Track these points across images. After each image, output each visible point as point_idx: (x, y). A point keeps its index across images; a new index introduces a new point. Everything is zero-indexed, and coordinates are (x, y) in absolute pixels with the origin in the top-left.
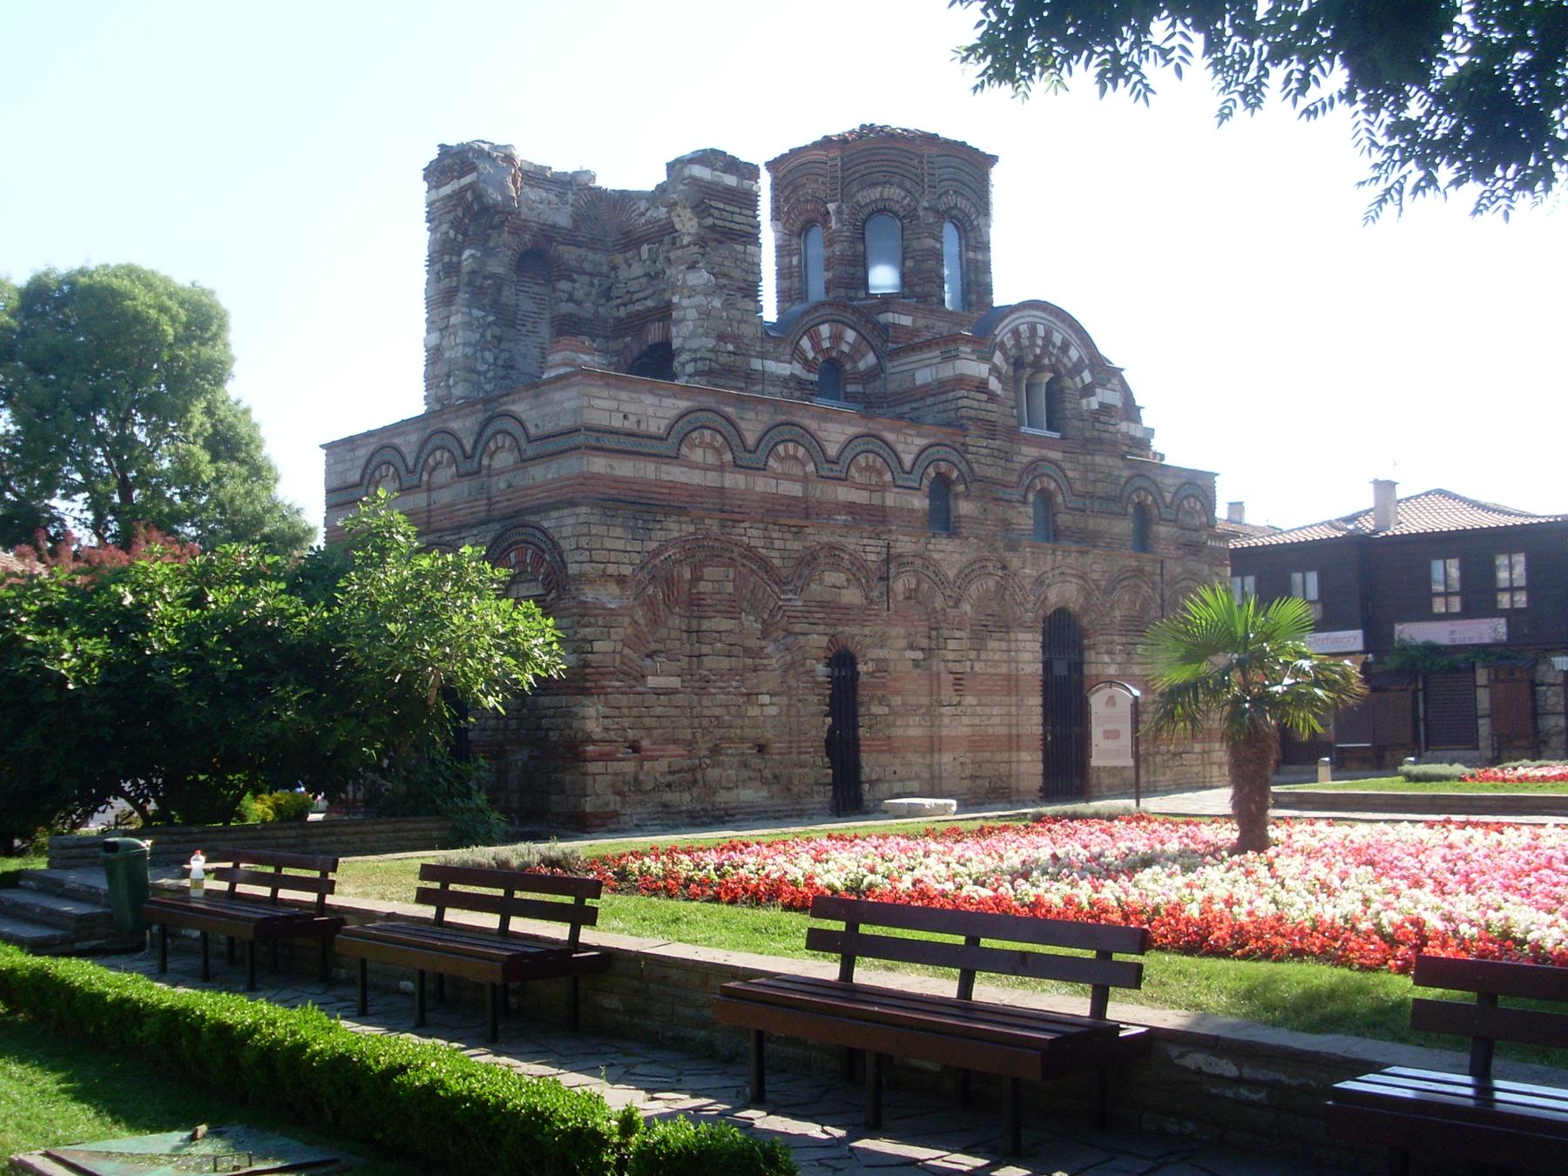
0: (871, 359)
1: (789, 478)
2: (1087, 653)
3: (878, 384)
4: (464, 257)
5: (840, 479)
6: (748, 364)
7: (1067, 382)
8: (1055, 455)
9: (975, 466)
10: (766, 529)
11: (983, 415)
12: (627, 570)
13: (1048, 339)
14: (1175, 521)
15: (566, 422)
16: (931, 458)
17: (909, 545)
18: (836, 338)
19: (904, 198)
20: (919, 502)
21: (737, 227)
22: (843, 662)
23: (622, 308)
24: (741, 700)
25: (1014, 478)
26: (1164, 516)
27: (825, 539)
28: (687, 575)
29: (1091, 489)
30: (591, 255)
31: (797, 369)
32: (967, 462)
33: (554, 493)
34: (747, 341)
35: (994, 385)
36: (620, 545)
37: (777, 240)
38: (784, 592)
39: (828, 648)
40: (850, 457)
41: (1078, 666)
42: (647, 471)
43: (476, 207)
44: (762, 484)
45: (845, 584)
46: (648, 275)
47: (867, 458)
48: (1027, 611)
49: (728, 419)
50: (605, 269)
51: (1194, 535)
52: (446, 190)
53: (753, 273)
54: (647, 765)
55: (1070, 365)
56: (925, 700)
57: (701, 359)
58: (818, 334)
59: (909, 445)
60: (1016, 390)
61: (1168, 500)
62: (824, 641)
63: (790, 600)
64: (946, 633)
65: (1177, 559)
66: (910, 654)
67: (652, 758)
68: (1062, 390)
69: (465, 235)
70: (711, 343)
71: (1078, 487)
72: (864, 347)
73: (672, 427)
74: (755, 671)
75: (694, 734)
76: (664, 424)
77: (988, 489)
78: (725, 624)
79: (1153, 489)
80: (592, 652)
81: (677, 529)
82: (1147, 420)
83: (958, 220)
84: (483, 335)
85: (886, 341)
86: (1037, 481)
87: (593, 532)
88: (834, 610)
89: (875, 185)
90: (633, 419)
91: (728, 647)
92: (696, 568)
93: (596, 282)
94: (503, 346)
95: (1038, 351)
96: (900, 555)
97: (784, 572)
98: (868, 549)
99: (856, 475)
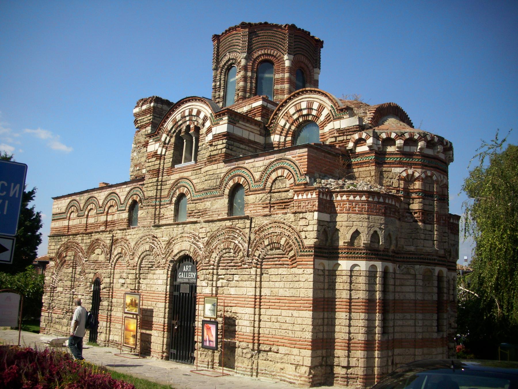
5: (101, 213)
9: (145, 193)
12: (54, 255)
14: (264, 189)
20: (125, 215)
21: (144, 123)
22: (97, 283)
26: (252, 189)
34: (143, 163)
48: (164, 258)
51: (284, 195)
71: (199, 187)
74: (78, 286)
79: (245, 173)
90: (60, 209)
95: (188, 123)
96: (117, 240)
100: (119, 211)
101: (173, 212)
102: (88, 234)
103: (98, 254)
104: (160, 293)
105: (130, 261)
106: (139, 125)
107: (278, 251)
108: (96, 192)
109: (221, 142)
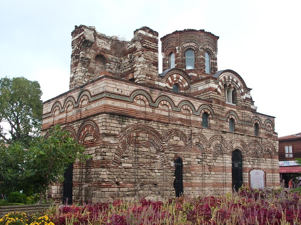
0: (187, 84)
1: (164, 110)
2: (243, 161)
3: (188, 90)
4: (80, 54)
6: (154, 83)
7: (237, 91)
8: (235, 110)
9: (215, 112)
10: (158, 124)
11: (216, 98)
12: (117, 133)
13: (232, 80)
14: (265, 129)
15: (101, 90)
16: (203, 108)
17: (197, 130)
18: (178, 78)
19: (195, 46)
20: (200, 119)
21: (152, 47)
22: (178, 161)
23: (123, 71)
24: (150, 171)
25: (224, 115)
26: (262, 127)
27: (174, 127)
28: (135, 135)
29: (244, 119)
30: (115, 58)
31: (167, 85)
32: (213, 110)
33: (97, 111)
34: (154, 77)
35: (219, 90)
36: (115, 125)
37: (163, 57)
38: (162, 141)
39: (175, 157)
40: (181, 106)
41: (241, 165)
42: (124, 105)
43: (83, 40)
44: (157, 111)
45: (179, 140)
46: (129, 62)
47: (186, 106)
48: (228, 149)
49: (148, 93)
50: (119, 61)
51: (269, 132)
52: (77, 37)
53: (156, 59)
54: (121, 189)
55: (238, 87)
56: (201, 173)
57: (142, 80)
58: (173, 77)
59: (197, 104)
60: (225, 93)
61: (263, 123)
62: (173, 155)
63: (164, 144)
64: (207, 155)
65: (265, 139)
66: (197, 160)
67: (123, 187)
68: (236, 93)
69: (81, 48)
70: (144, 76)
71: (240, 118)
72: (185, 81)
73: (132, 94)
74: (154, 163)
75: (135, 180)
76: (129, 93)
77: (217, 117)
78: (145, 149)
80: (106, 156)
81: (132, 122)
82: (255, 104)
83: (209, 52)
84: (85, 74)
85: (190, 80)
86: (230, 116)
87: (107, 121)
88: (176, 147)
89: (188, 42)
90: (120, 91)
91: (146, 156)
92: (137, 133)
93: (116, 64)
94: (90, 78)
95: (230, 83)
96: (194, 133)
97: (163, 136)
98: (186, 131)
99: (183, 111)
100: (194, 115)
101: (229, 126)
102: (165, 123)
103: (176, 140)
104: (229, 167)
105: (207, 148)
106: (148, 46)
107: (268, 152)
108: (170, 94)
109: (249, 102)
